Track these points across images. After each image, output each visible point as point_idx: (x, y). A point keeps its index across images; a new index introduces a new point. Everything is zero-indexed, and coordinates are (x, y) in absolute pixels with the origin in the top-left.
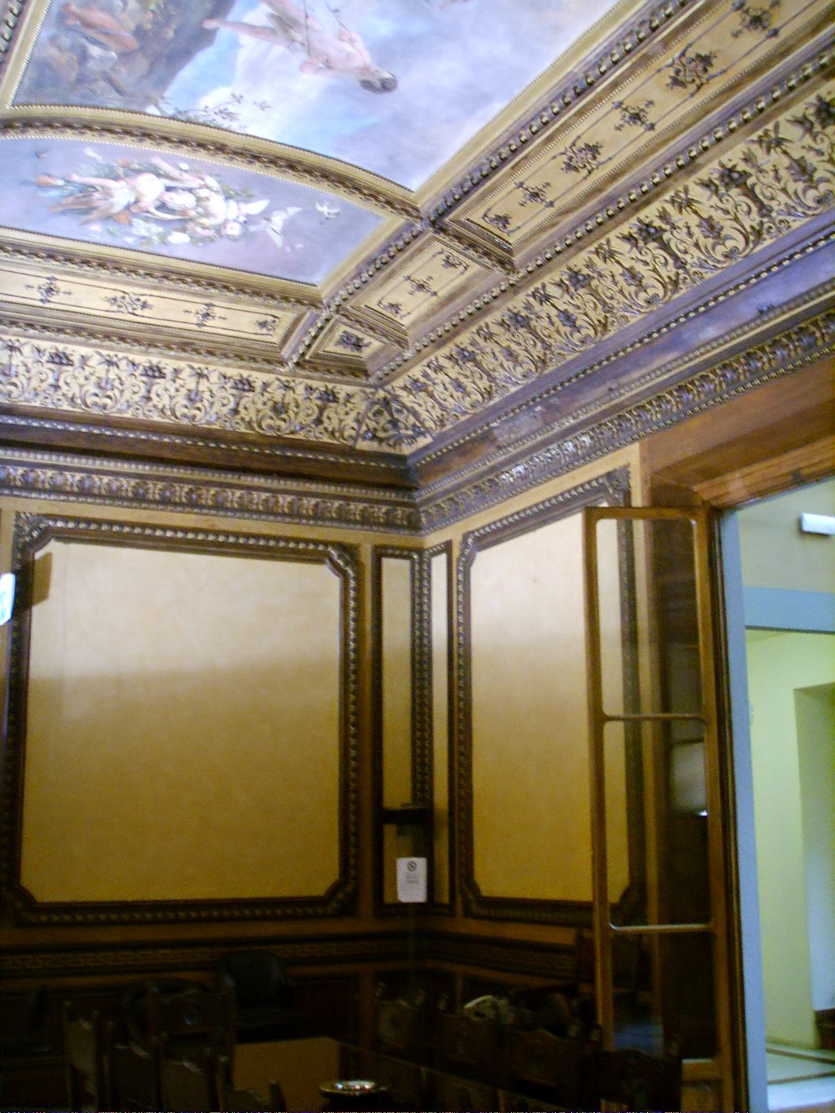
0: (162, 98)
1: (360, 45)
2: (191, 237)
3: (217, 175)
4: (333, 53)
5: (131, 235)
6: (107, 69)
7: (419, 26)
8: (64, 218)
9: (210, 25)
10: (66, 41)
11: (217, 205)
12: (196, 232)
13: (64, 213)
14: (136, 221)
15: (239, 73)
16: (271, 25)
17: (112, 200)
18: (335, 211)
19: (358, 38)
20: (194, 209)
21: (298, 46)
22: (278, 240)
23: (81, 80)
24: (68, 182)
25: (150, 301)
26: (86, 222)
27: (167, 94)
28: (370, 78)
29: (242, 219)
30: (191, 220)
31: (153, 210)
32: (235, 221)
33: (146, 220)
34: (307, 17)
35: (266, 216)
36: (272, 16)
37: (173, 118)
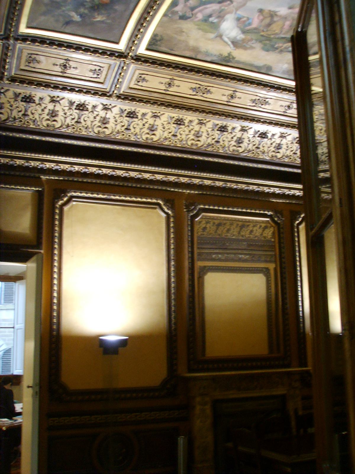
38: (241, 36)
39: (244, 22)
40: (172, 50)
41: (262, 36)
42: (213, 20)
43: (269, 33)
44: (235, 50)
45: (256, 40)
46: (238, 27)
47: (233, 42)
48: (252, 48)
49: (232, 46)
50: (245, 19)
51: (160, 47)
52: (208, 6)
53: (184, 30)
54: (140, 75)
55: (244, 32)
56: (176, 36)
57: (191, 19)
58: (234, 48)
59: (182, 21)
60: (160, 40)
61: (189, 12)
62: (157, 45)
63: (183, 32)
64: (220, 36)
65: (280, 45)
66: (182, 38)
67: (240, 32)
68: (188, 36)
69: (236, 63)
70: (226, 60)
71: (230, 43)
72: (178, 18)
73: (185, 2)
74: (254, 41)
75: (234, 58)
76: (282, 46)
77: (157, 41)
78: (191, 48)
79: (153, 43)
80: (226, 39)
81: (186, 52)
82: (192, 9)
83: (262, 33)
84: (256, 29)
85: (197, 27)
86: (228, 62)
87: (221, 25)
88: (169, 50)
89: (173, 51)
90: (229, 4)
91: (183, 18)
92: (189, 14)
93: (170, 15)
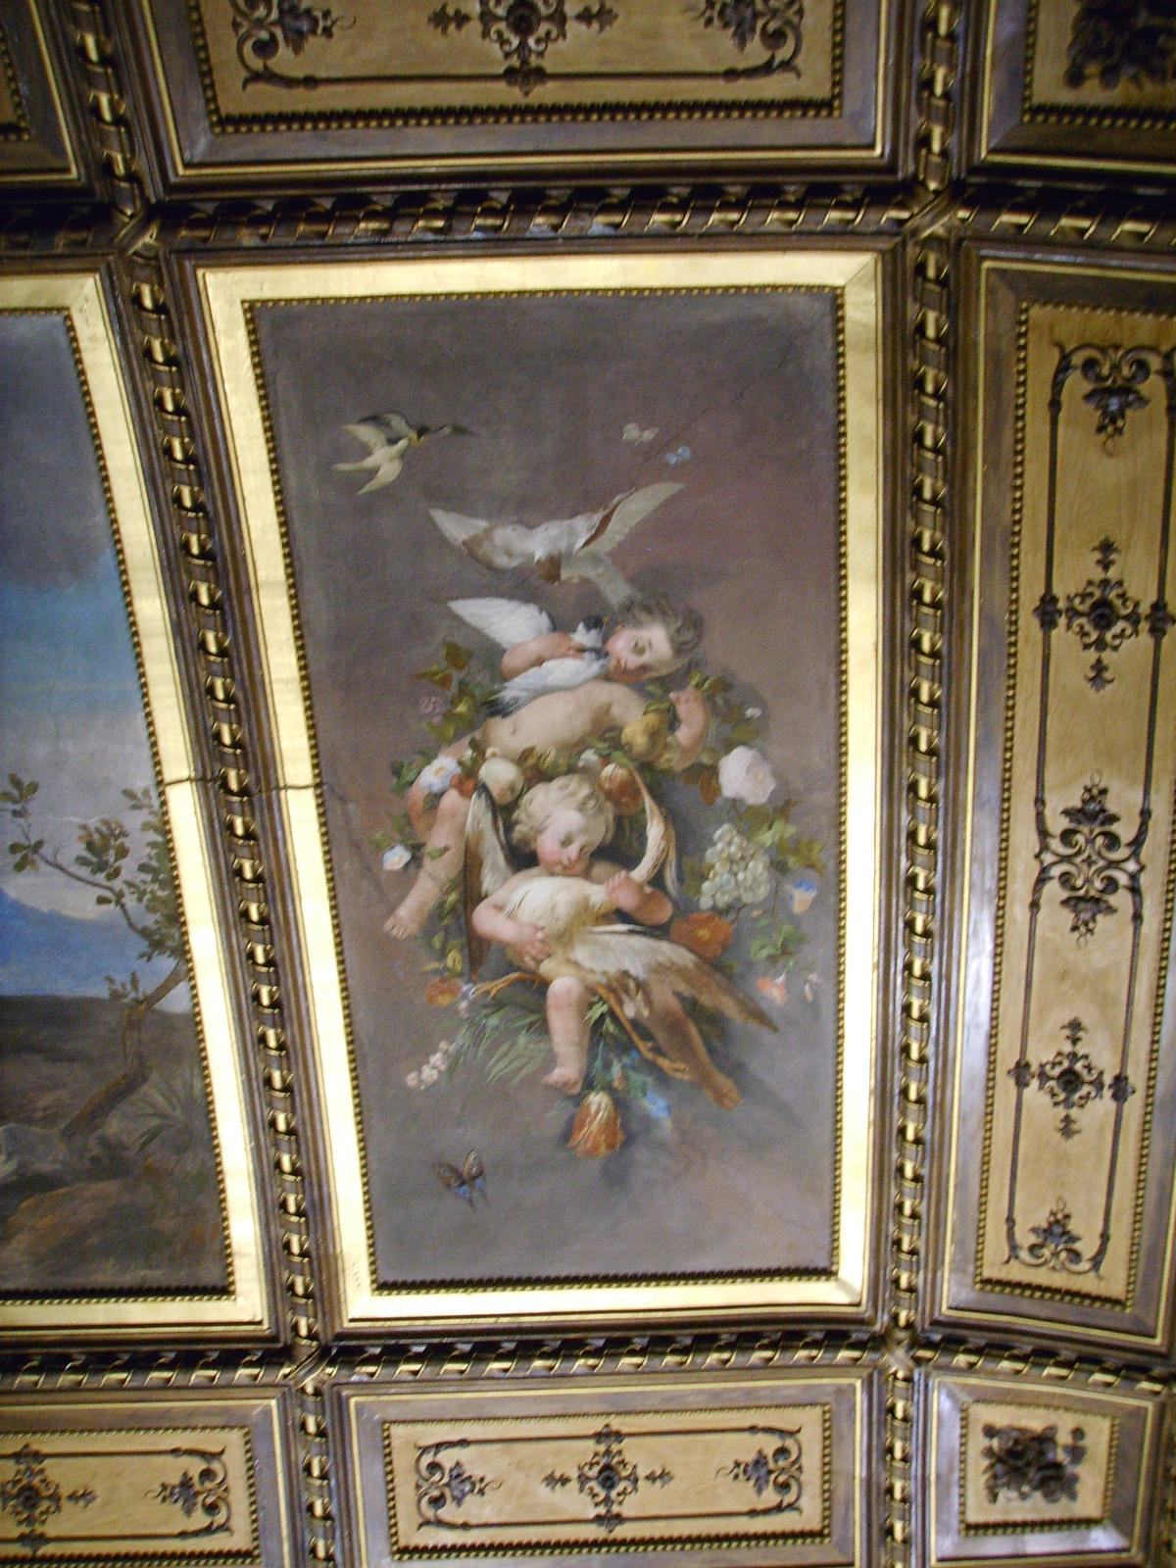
0: (116, 996)
2: (729, 746)
3: (397, 772)
5: (776, 903)
6: (55, 1132)
8: (756, 1066)
11: (540, 721)
12: (700, 739)
13: (736, 1071)
14: (711, 894)
17: (637, 969)
18: (366, 433)
20: (589, 773)
22: (636, 508)
24: (589, 1085)
25: (1064, 797)
26: (760, 1016)
27: (102, 992)
29: (582, 636)
30: (646, 766)
31: (641, 872)
32: (600, 653)
33: (694, 875)
35: (531, 584)
37: (182, 952)
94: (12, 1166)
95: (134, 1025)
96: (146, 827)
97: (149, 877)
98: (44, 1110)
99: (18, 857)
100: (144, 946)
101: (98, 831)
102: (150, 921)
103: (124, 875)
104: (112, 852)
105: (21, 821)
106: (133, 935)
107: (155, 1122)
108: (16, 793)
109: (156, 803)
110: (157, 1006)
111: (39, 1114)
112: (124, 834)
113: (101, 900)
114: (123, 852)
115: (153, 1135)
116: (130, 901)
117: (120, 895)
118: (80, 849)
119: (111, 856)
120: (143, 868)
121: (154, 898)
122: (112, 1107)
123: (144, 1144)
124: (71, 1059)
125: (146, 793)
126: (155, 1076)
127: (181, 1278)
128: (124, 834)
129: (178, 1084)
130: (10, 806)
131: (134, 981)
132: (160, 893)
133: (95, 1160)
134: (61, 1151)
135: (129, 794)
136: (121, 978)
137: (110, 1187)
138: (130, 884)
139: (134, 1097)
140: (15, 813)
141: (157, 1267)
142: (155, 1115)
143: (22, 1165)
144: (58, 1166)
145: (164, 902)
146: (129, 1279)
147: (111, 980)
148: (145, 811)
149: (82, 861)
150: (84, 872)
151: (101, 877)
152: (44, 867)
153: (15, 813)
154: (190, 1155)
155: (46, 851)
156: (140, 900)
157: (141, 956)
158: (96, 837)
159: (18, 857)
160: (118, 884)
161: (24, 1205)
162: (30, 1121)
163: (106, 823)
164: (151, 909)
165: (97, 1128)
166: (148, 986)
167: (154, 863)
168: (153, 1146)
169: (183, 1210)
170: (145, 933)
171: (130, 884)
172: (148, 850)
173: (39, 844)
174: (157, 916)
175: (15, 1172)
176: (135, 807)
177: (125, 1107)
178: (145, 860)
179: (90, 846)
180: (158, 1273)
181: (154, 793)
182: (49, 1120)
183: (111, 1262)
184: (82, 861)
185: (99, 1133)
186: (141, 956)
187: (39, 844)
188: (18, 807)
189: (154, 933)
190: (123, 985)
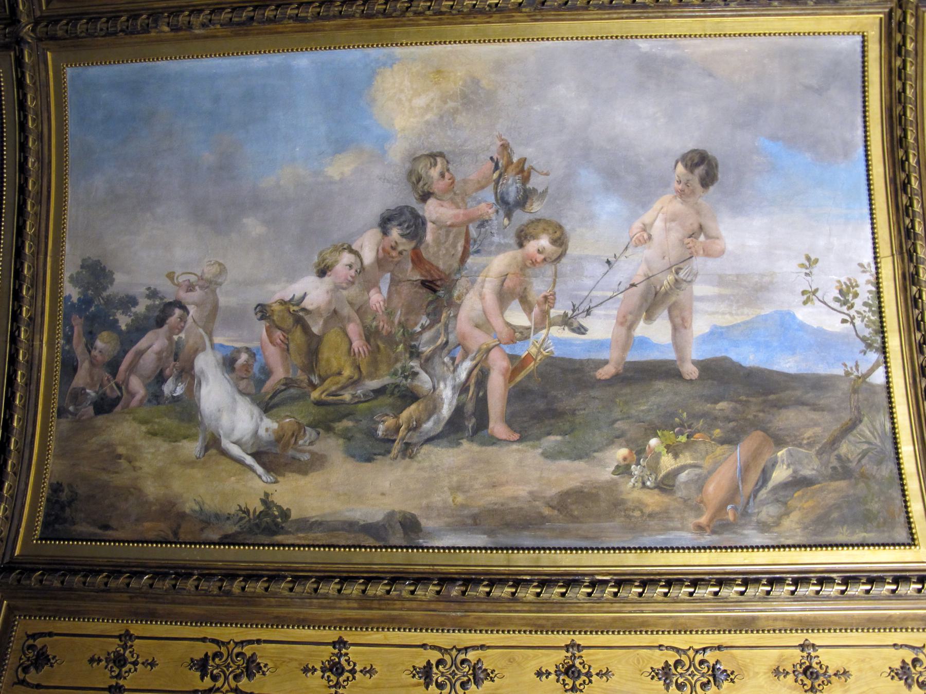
0: (848, 374)
1: (647, 218)
4: (675, 235)
6: (813, 452)
7: (588, 178)
9: (690, 371)
10: (768, 512)
15: (767, 310)
16: (666, 312)
19: (637, 225)
21: (682, 275)
23: (843, 471)
27: (840, 372)
28: (695, 181)
34: (633, 285)
36: (649, 318)
37: (884, 350)
38: (268, 426)
39: (247, 367)
40: (106, 527)
41: (319, 403)
42: (175, 391)
43: (331, 385)
44: (276, 482)
45: (313, 425)
46: (242, 393)
47: (256, 455)
48: (318, 462)
49: (260, 470)
50: (244, 357)
51: (74, 523)
52: (142, 344)
53: (121, 450)
54: (31, 642)
55: (267, 407)
56: (105, 477)
57: (121, 403)
58: (270, 478)
59: (100, 420)
60: (70, 503)
61: (108, 380)
62: (65, 521)
63: (120, 456)
64: (213, 443)
65: (390, 422)
66: (122, 479)
67: (256, 411)
68: (134, 469)
69: (298, 530)
70: (264, 525)
71: (249, 460)
72: (91, 410)
73: (90, 352)
74: (310, 433)
75: (285, 514)
76: (397, 429)
77: (63, 508)
78: (154, 508)
79: (53, 517)
80: (236, 450)
81: (147, 525)
82: (113, 366)
83: (315, 395)
84: (288, 383)
85: (144, 428)
86: (275, 533)
87: (199, 399)
88: (99, 531)
89: (113, 529)
90: (183, 319)
91: (105, 406)
92: (111, 391)
93: (71, 408)
94: (790, 471)
95: (855, 391)
96: (868, 282)
97: (867, 309)
98: (808, 438)
99: (805, 297)
100: (862, 346)
101: (845, 283)
102: (867, 332)
103: (856, 308)
104: (851, 295)
105: (808, 278)
106: (858, 340)
107: (865, 446)
108: (807, 264)
109: (874, 271)
110: (868, 380)
111: (805, 442)
112: (857, 286)
113: (844, 321)
114: (856, 295)
115: (864, 454)
116: (858, 321)
117: (853, 318)
118: (836, 293)
119: (850, 297)
120: (865, 304)
121: (870, 320)
122: (843, 438)
123: (859, 461)
124: (822, 410)
125: (869, 265)
126: (866, 419)
127: (884, 538)
128: (857, 286)
129: (878, 426)
130: (804, 271)
131: (857, 366)
132: (872, 318)
133: (834, 468)
134: (816, 463)
135: (861, 265)
136: (851, 364)
137: (842, 484)
138: (858, 313)
139: (855, 432)
140: (807, 274)
141: (870, 532)
142: (865, 442)
143: (795, 472)
144: (814, 472)
145: (874, 322)
146: (855, 539)
147: (846, 366)
148: (868, 274)
149: (836, 300)
150: (836, 305)
151: (844, 309)
152: (817, 303)
153: (807, 274)
154: (884, 467)
155: (819, 294)
156: (862, 321)
157: (861, 352)
158: (844, 286)
159: (805, 297)
160: (852, 312)
161: (796, 495)
162: (800, 445)
163: (849, 280)
164: (867, 326)
165: (836, 449)
166: (863, 369)
167: (870, 302)
168: (863, 461)
169: (882, 498)
170: (864, 339)
171: (858, 313)
172: (868, 294)
173: (817, 290)
174: (870, 330)
175: (790, 476)
176: (864, 272)
177: (850, 437)
178: (866, 300)
179: (841, 292)
180: (872, 535)
181: (873, 266)
182: (810, 445)
183: (845, 528)
184: (836, 300)
185: (836, 453)
186: (861, 352)
187: (817, 290)
188: (807, 271)
189: (868, 339)
190: (851, 368)
